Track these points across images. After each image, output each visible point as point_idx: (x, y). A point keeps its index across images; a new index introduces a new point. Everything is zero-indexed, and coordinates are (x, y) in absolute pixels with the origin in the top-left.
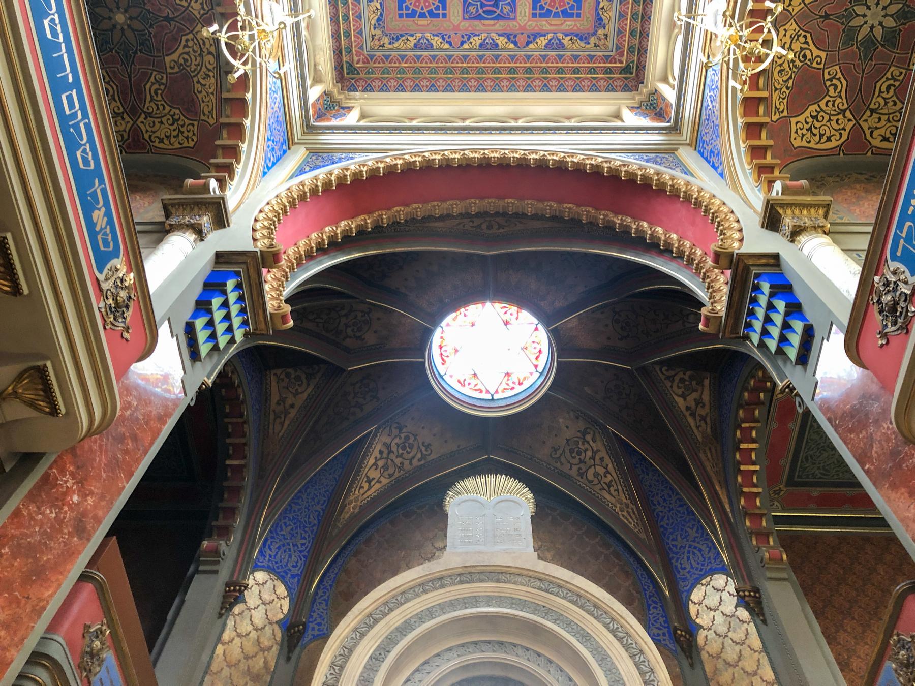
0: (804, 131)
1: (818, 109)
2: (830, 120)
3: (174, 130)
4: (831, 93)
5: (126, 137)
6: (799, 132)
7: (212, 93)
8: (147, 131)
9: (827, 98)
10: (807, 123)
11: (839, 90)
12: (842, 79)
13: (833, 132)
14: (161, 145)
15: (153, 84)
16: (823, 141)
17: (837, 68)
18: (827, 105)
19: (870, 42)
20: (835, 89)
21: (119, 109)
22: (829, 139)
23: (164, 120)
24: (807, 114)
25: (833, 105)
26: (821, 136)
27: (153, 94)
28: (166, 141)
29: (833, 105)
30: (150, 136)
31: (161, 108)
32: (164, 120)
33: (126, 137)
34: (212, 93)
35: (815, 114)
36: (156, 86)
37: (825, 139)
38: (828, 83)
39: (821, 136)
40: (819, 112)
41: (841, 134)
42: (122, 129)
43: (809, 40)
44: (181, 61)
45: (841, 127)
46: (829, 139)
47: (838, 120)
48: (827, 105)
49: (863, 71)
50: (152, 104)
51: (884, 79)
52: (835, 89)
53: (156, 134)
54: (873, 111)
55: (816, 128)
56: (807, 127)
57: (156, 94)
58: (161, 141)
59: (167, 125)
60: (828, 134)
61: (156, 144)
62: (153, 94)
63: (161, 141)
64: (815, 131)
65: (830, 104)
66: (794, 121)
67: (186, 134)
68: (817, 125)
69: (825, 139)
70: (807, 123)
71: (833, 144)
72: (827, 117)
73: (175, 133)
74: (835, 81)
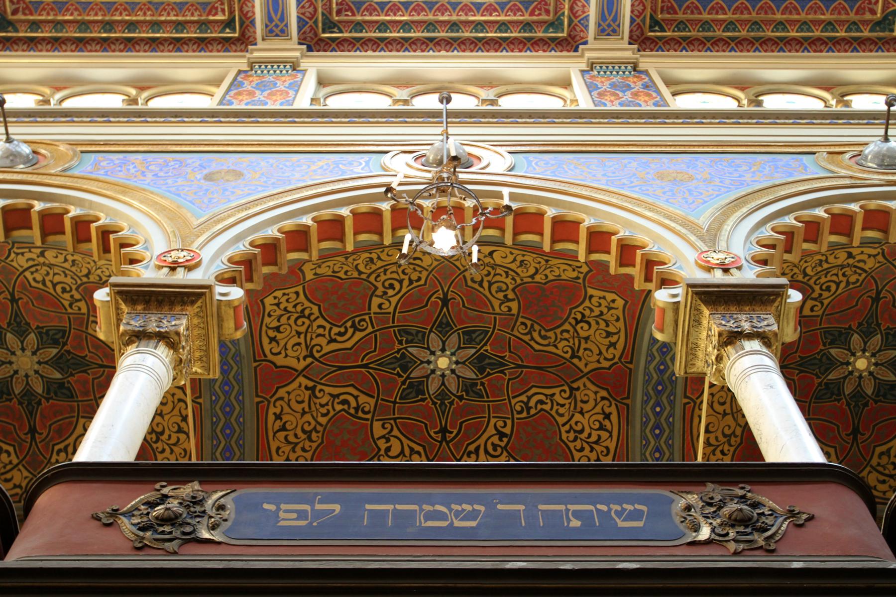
1: (312, 318)
2: (299, 334)
4: (336, 330)
9: (328, 326)
10: (295, 306)
11: (339, 338)
18: (319, 327)
19: (405, 363)
20: (340, 334)
25: (319, 335)
26: (277, 329)
29: (319, 335)
35: (307, 312)
37: (272, 334)
38: (349, 324)
39: (277, 329)
40: (308, 318)
41: (280, 353)
45: (290, 352)
46: (272, 339)
48: (319, 327)
49: (365, 366)
51: (356, 393)
52: (340, 334)
54: (313, 389)
56: (290, 309)
60: (279, 336)
64: (284, 320)
65: (321, 331)
66: (300, 289)
68: (292, 321)
69: (272, 334)
70: (295, 306)
71: (267, 347)
72: (302, 329)
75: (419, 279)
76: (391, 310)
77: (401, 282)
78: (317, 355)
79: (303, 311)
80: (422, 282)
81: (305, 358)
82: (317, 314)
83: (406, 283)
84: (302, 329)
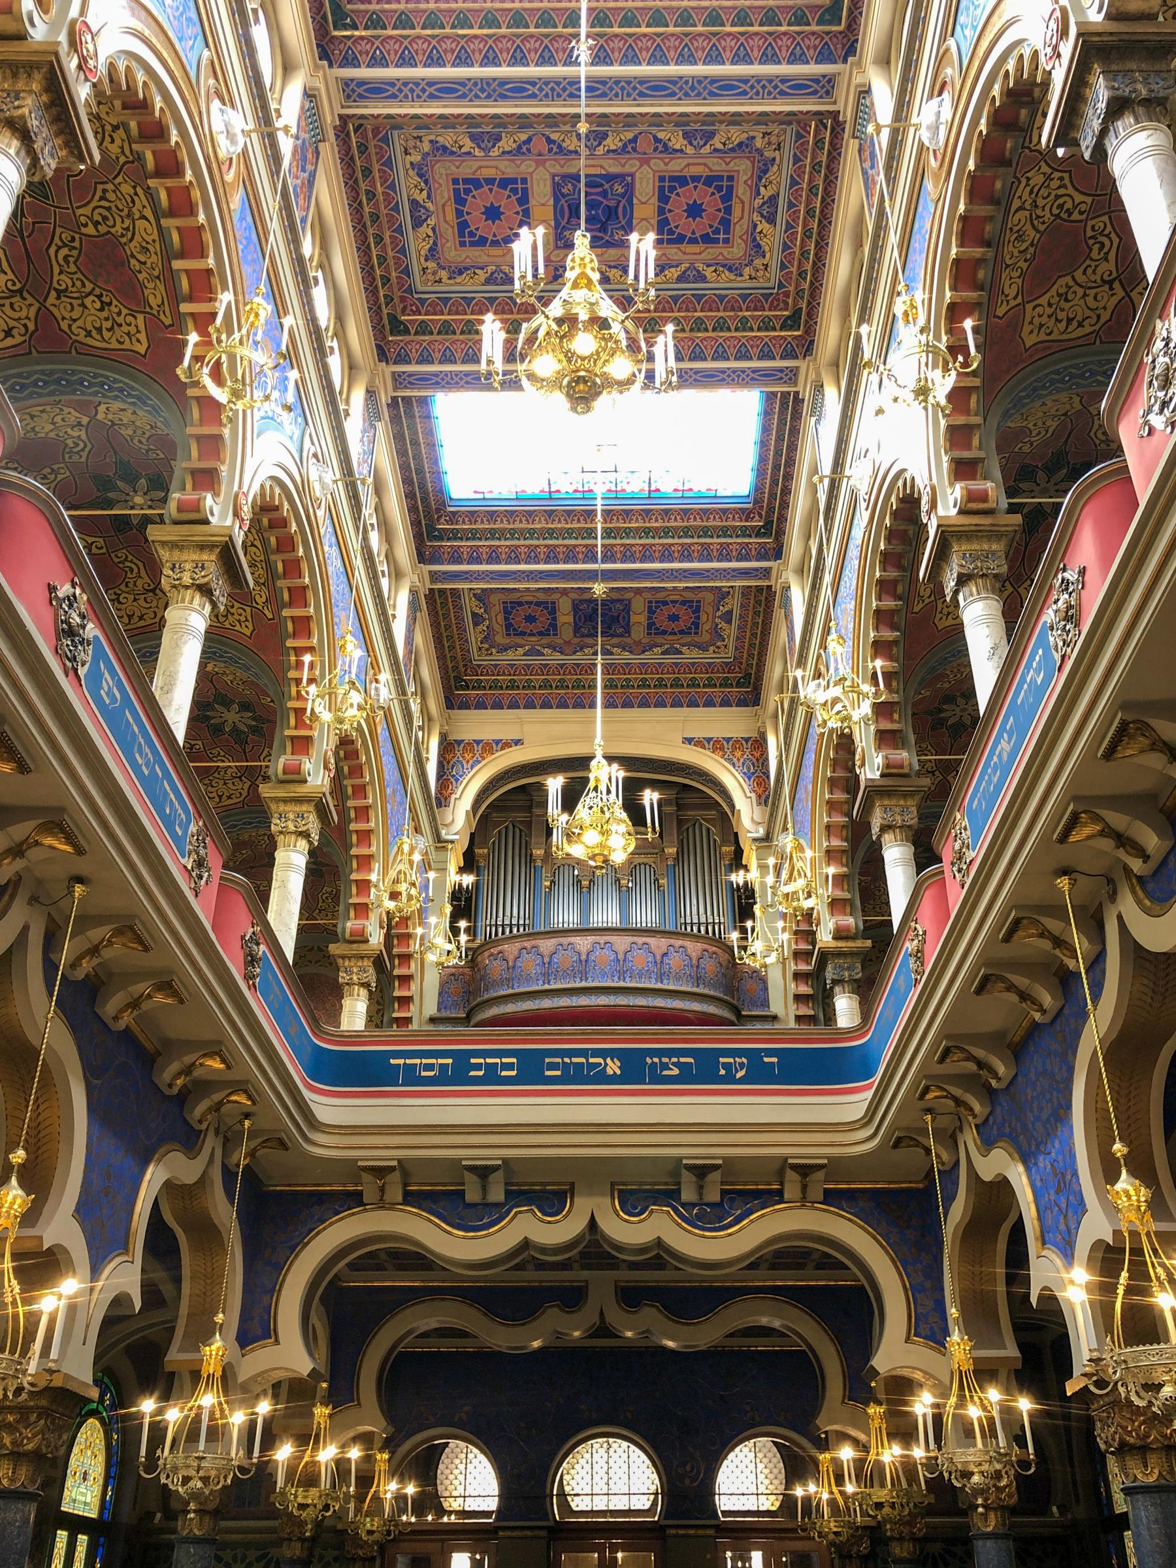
0: (1044, 320)
1: (1071, 283)
2: (1085, 295)
3: (107, 319)
5: (31, 327)
6: (1037, 321)
7: (158, 277)
8: (63, 318)
12: (1113, 235)
13: (1088, 313)
14: (89, 341)
15: (59, 248)
16: (1071, 328)
17: (1105, 218)
20: (1100, 250)
21: (14, 284)
22: (1080, 325)
23: (88, 301)
24: (1053, 292)
27: (62, 263)
28: (94, 333)
30: (70, 326)
31: (78, 284)
32: (88, 301)
33: (31, 327)
34: (158, 277)
35: (1062, 291)
36: (64, 251)
37: (1075, 323)
41: (1099, 317)
42: (23, 314)
43: (1067, 181)
44: (97, 218)
47: (1096, 295)
48: (1084, 273)
50: (63, 277)
53: (78, 323)
55: (1062, 310)
57: (68, 262)
58: (89, 334)
59: (93, 311)
60: (1079, 318)
61: (81, 338)
62: (62, 263)
63: (89, 334)
64: (1062, 315)
66: (1029, 307)
67: (125, 328)
69: (1075, 323)
71: (1088, 329)
73: (109, 324)
74: (1101, 239)
75: (1061, 179)
76: (1089, 200)
77: (1058, 197)
78: (1114, 275)
79: (1059, 295)
80: (1066, 175)
81: (1111, 289)
82: (1068, 279)
83: (1062, 191)
84: (1080, 292)
